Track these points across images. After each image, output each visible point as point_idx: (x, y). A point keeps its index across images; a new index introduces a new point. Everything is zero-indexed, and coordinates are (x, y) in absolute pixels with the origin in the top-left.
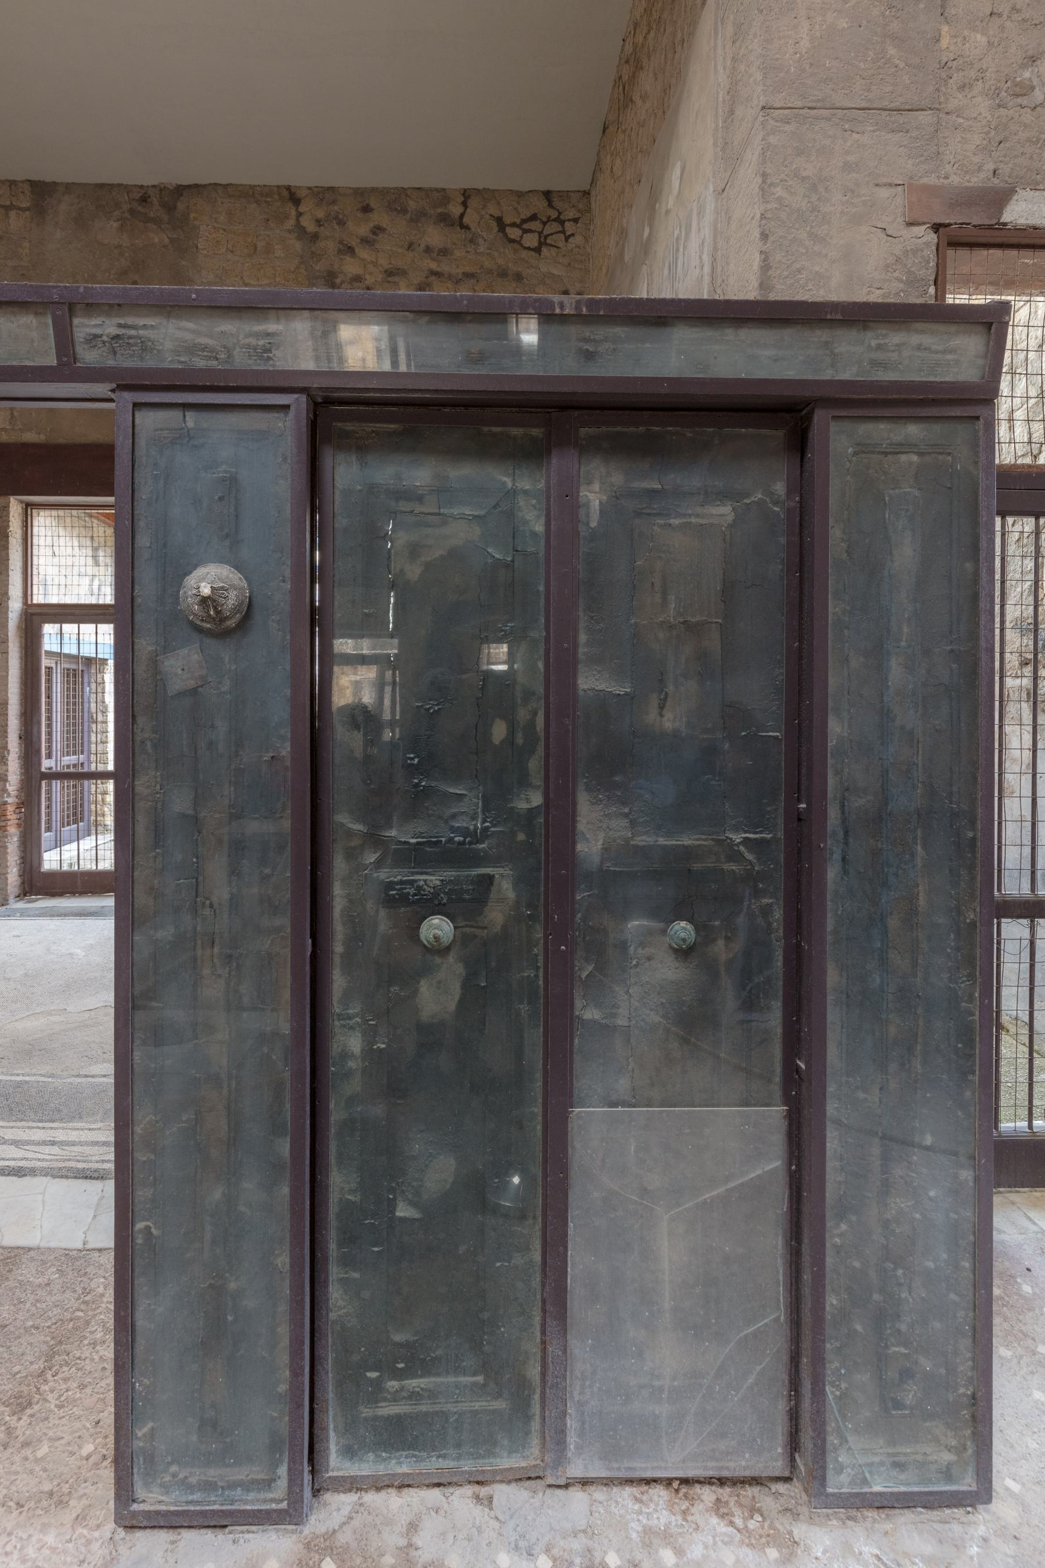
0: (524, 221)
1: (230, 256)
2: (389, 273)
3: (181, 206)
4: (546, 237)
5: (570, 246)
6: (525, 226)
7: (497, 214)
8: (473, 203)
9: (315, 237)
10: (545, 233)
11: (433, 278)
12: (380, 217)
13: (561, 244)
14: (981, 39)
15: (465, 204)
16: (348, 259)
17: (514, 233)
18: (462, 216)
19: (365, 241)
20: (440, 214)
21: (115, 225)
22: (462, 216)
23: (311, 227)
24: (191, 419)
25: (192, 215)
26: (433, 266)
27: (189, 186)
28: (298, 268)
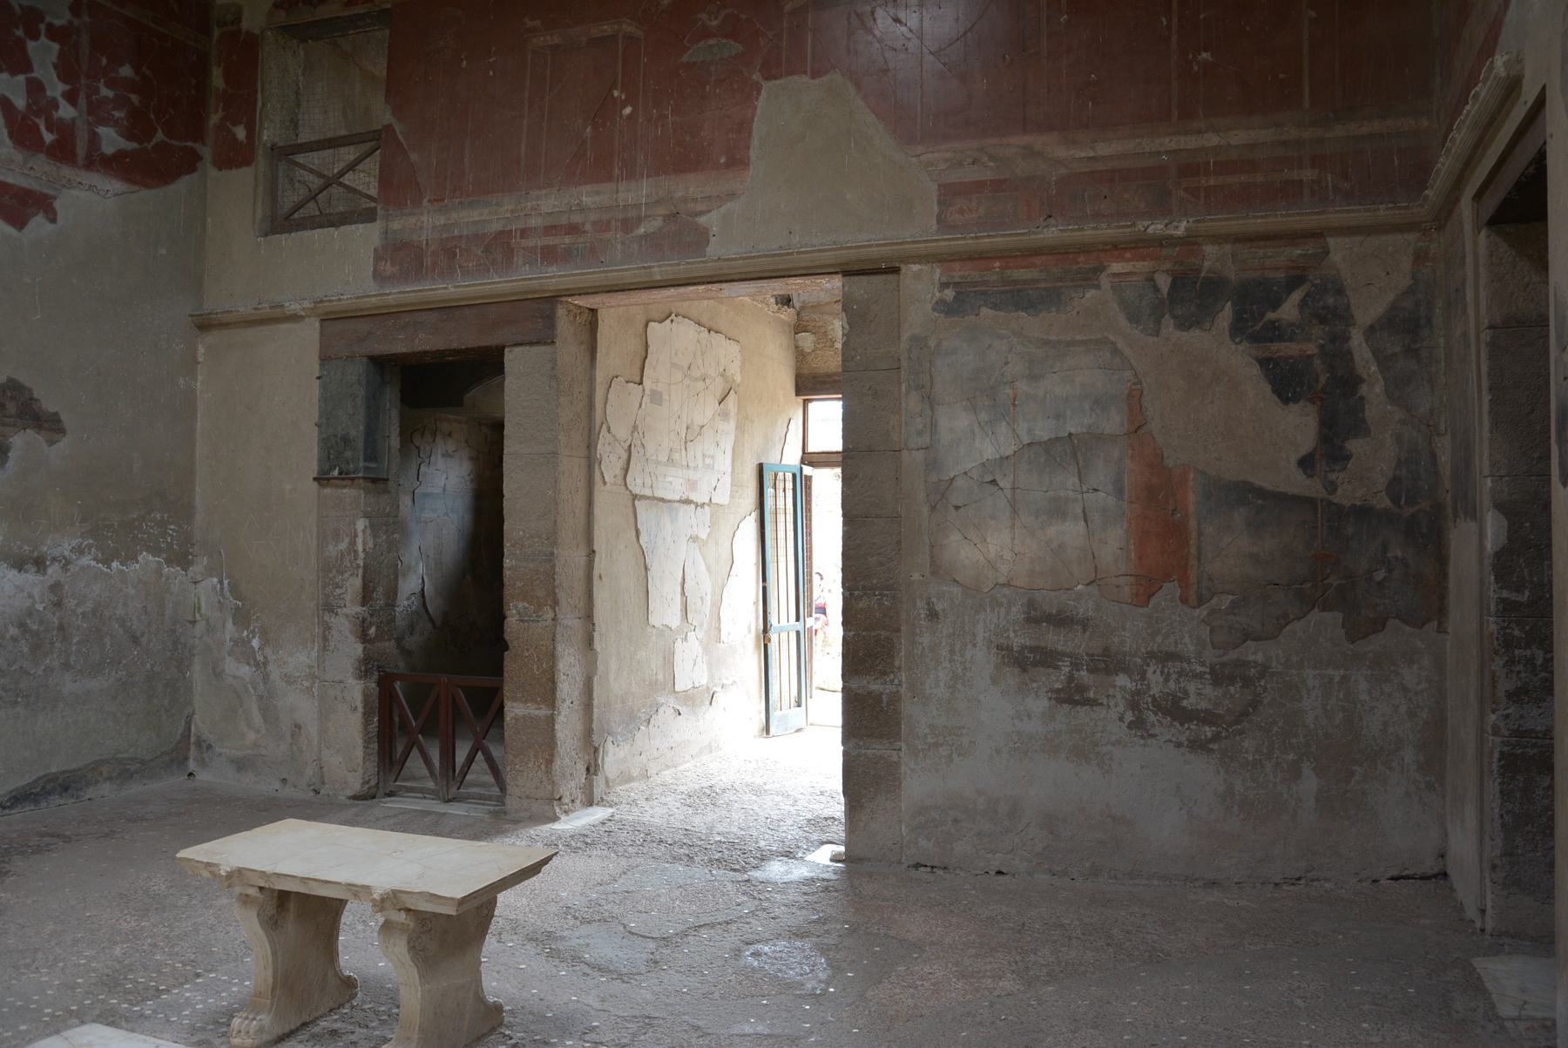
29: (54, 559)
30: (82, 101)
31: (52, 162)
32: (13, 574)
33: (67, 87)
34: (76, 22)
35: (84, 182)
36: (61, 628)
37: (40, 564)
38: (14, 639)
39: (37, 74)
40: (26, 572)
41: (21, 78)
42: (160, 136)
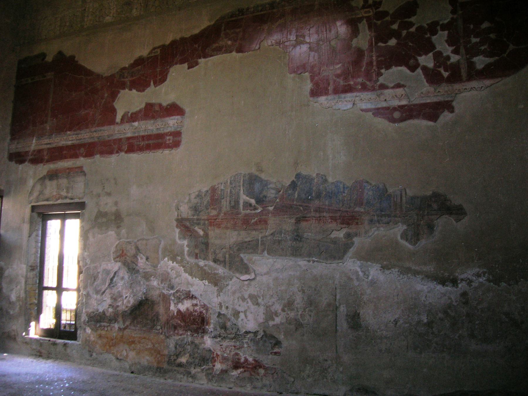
29: (462, 280)
30: (462, 50)
31: (449, 85)
32: (439, 287)
33: (454, 48)
34: (455, 16)
35: (467, 88)
36: (468, 315)
37: (454, 282)
38: (441, 320)
39: (438, 48)
40: (447, 286)
41: (431, 54)
42: (511, 47)
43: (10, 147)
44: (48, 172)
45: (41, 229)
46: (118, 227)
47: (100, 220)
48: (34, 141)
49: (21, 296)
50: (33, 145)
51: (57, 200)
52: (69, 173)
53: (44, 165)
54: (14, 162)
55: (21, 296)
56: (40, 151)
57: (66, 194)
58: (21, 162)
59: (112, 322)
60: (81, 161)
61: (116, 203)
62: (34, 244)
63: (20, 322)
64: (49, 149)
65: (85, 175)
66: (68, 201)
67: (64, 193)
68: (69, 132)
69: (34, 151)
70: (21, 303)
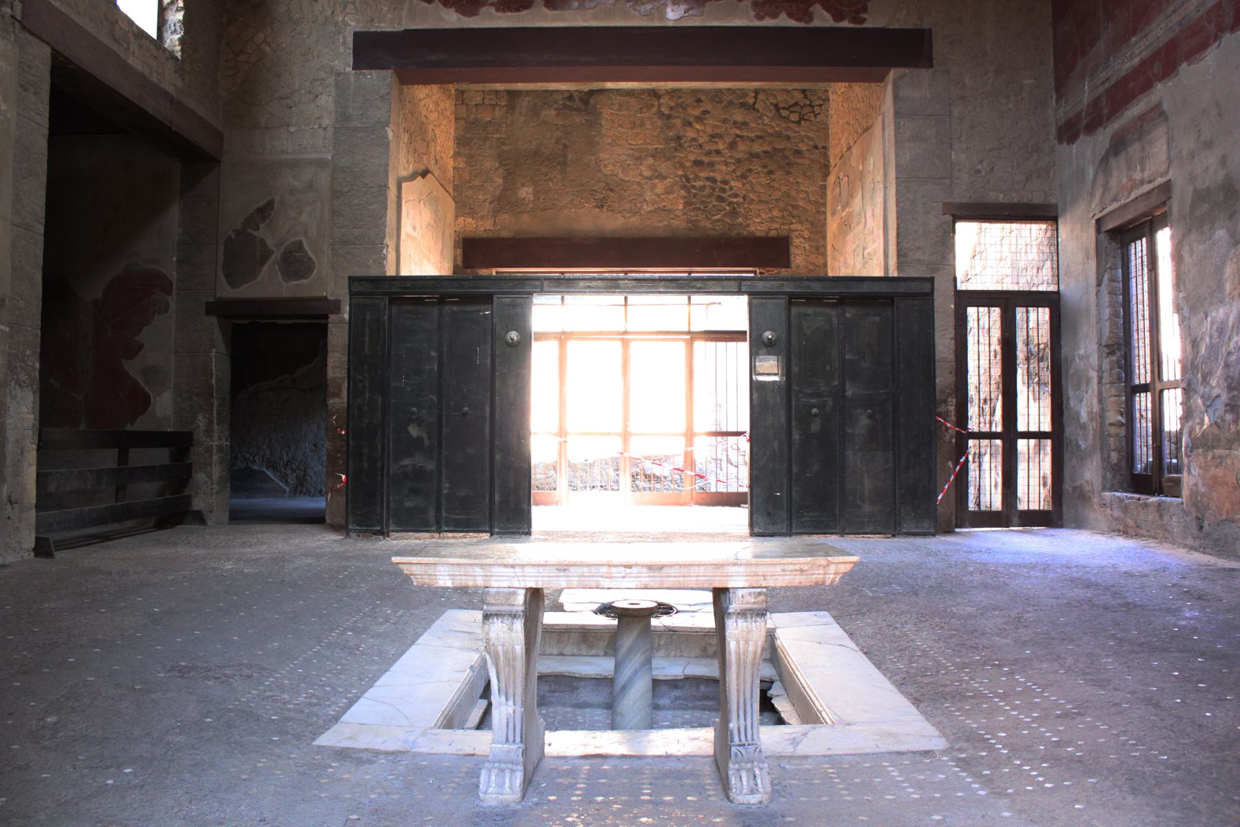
0: (790, 106)
1: (620, 129)
2: (712, 136)
3: (592, 101)
4: (803, 115)
5: (818, 120)
6: (792, 109)
7: (774, 101)
8: (760, 97)
9: (669, 117)
10: (803, 113)
11: (738, 139)
12: (708, 106)
13: (812, 119)
14: (964, 156)
15: (756, 97)
16: (688, 128)
17: (784, 113)
18: (755, 103)
19: (699, 119)
20: (741, 103)
21: (554, 112)
22: (755, 103)
23: (667, 112)
24: (764, 301)
25: (598, 106)
26: (738, 132)
27: (596, 90)
28: (659, 134)
43: (1058, 116)
44: (1112, 138)
45: (1120, 266)
46: (1231, 217)
47: (1198, 213)
48: (1086, 87)
49: (1094, 410)
50: (1086, 95)
51: (1129, 194)
52: (1142, 127)
53: (1105, 128)
54: (1065, 143)
55: (1094, 410)
56: (1095, 103)
57: (1141, 175)
58: (1072, 139)
59: (1233, 447)
60: (1161, 91)
61: (1223, 161)
62: (1106, 298)
63: (1095, 463)
64: (1107, 91)
65: (1166, 119)
66: (1147, 188)
67: (1137, 176)
68: (1134, 39)
69: (1088, 106)
70: (1094, 424)
